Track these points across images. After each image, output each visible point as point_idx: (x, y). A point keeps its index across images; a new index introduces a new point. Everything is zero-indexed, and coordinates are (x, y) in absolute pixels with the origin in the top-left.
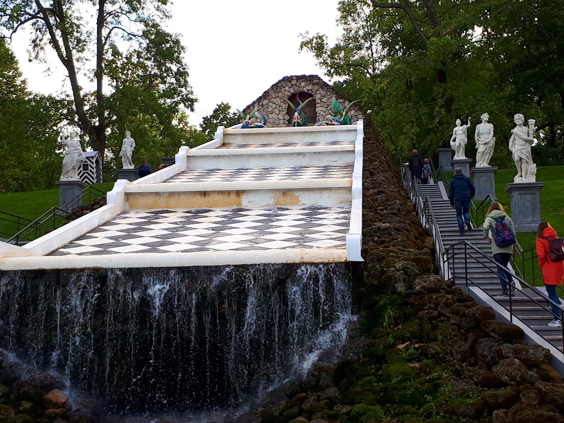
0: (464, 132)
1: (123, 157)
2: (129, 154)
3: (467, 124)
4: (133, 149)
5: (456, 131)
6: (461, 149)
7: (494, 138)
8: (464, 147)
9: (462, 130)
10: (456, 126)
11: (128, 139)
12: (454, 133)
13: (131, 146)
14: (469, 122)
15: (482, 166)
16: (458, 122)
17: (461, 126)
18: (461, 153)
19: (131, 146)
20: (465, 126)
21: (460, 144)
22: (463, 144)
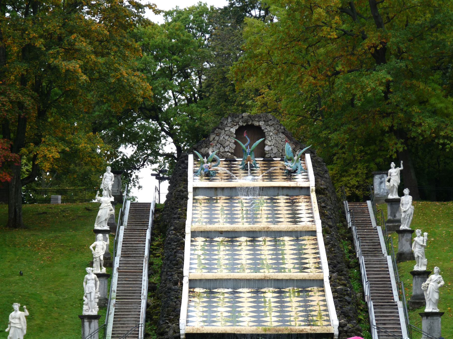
0: (397, 174)
1: (104, 189)
3: (400, 167)
4: (113, 183)
5: (391, 173)
6: (395, 190)
8: (397, 187)
9: (396, 172)
10: (390, 168)
11: (109, 173)
13: (111, 180)
14: (402, 165)
15: (404, 228)
16: (393, 165)
17: (395, 168)
18: (394, 193)
19: (111, 180)
20: (398, 169)
22: (396, 185)
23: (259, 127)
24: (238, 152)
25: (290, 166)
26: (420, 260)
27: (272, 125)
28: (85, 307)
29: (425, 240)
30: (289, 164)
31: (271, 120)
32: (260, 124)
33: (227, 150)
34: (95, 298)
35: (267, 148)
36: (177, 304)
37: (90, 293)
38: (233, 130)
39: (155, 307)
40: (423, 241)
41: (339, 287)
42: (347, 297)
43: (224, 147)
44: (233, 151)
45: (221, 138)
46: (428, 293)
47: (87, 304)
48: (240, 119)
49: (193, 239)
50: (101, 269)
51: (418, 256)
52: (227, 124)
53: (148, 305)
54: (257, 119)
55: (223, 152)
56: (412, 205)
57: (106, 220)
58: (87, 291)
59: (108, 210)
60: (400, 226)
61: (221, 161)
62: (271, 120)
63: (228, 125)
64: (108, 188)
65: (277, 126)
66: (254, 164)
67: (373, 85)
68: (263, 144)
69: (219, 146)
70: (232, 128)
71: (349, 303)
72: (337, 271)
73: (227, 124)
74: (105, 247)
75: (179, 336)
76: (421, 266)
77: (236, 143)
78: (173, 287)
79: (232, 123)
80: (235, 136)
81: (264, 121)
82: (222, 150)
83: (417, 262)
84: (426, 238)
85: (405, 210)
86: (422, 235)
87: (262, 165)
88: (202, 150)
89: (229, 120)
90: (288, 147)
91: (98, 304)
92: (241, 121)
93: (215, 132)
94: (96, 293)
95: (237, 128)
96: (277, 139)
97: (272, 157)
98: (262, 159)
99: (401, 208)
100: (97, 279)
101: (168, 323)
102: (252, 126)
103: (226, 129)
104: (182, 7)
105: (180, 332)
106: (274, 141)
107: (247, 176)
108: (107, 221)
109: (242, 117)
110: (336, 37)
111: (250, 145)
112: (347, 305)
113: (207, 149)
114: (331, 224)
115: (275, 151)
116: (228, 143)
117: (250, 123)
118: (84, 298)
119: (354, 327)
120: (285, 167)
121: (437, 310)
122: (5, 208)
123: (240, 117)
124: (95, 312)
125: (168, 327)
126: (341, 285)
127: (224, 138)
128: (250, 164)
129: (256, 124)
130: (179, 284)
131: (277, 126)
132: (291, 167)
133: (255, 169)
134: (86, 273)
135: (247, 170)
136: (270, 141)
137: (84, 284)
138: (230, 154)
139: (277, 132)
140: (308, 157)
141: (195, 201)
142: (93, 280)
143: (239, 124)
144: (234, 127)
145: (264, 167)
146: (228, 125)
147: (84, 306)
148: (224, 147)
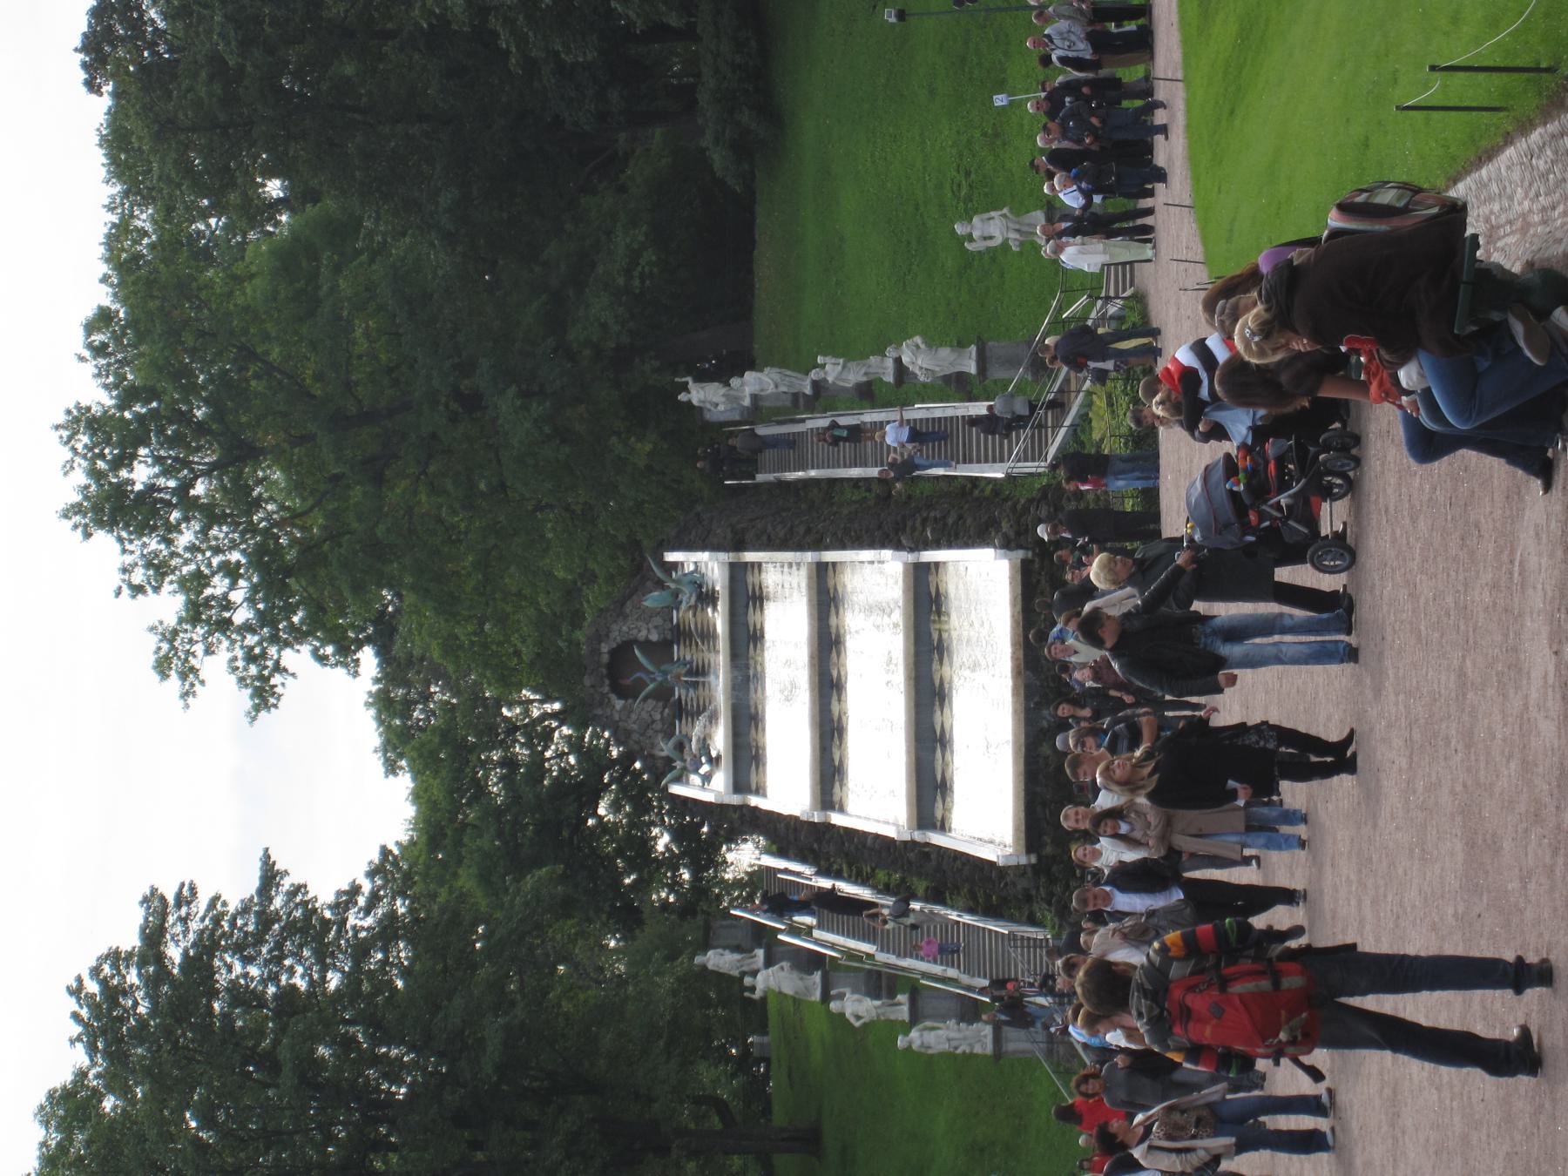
0: (702, 388)
2: (737, 956)
3: (687, 383)
4: (727, 952)
5: (700, 401)
7: (767, 370)
12: (701, 405)
16: (682, 397)
17: (689, 392)
20: (691, 385)
21: (723, 395)
23: (613, 653)
24: (663, 694)
25: (688, 597)
26: (872, 370)
27: (608, 628)
28: (978, 1049)
29: (833, 360)
30: (684, 598)
33: (658, 717)
34: (959, 1030)
35: (654, 637)
36: (969, 861)
37: (949, 1040)
38: (619, 704)
39: (973, 895)
40: (835, 364)
41: (929, 534)
42: (950, 521)
43: (653, 722)
44: (661, 704)
45: (635, 727)
46: (937, 369)
47: (971, 1045)
49: (837, 807)
50: (899, 1004)
51: (866, 374)
53: (971, 911)
55: (663, 725)
56: (762, 371)
57: (801, 979)
58: (946, 1047)
59: (782, 974)
60: (804, 394)
61: (680, 732)
63: (609, 714)
64: (739, 961)
66: (685, 665)
67: (527, 425)
68: (647, 646)
69: (650, 732)
71: (960, 517)
72: (897, 534)
73: (607, 717)
74: (856, 996)
75: (1033, 866)
76: (885, 369)
77: (645, 699)
78: (934, 863)
80: (630, 701)
82: (658, 726)
83: (877, 376)
84: (829, 360)
85: (772, 386)
86: (823, 366)
87: (688, 649)
90: (653, 600)
91: (970, 1022)
94: (948, 1028)
97: (670, 626)
98: (675, 647)
99: (769, 391)
100: (921, 1026)
101: (1006, 884)
102: (610, 666)
104: (376, 741)
105: (1025, 866)
107: (709, 683)
108: (805, 976)
109: (593, 686)
111: (648, 672)
112: (964, 522)
114: (802, 529)
115: (658, 621)
116: (644, 715)
117: (604, 671)
118: (959, 1051)
119: (1008, 516)
120: (690, 607)
121: (973, 348)
122: (782, 1161)
123: (592, 691)
124: (988, 1030)
125: (1014, 884)
126: (924, 530)
127: (634, 723)
128: (685, 675)
129: (605, 658)
130: (927, 850)
132: (691, 596)
133: (695, 664)
134: (909, 1049)
135: (697, 683)
136: (639, 631)
137: (930, 1052)
138: (667, 710)
140: (672, 557)
141: (761, 791)
142: (921, 1036)
145: (691, 645)
147: (975, 1051)
148: (653, 722)
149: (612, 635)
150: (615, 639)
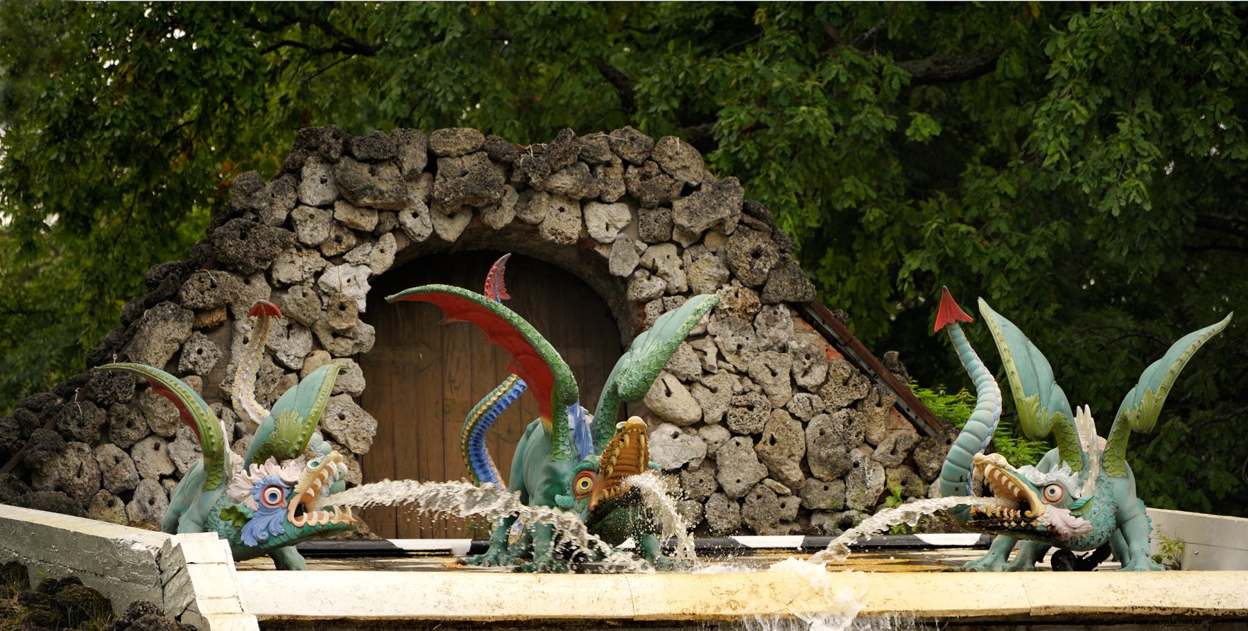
31: (687, 190)
32: (596, 228)
48: (413, 177)
52: (289, 224)
54: (563, 181)
62: (687, 190)
63: (306, 233)
65: (748, 244)
70: (338, 259)
73: (289, 224)
79: (342, 212)
81: (630, 199)
88: (73, 458)
89: (315, 187)
92: (418, 195)
93: (192, 292)
95: (389, 259)
96: (756, 365)
103: (284, 272)
106: (727, 384)
110: (542, 124)
113: (111, 450)
117: (502, 218)
131: (748, 244)
132: (1077, 510)
136: (689, 383)
139: (751, 298)
143: (399, 231)
144: (357, 255)
146: (306, 233)
149: (663, 256)
150: (654, 271)
